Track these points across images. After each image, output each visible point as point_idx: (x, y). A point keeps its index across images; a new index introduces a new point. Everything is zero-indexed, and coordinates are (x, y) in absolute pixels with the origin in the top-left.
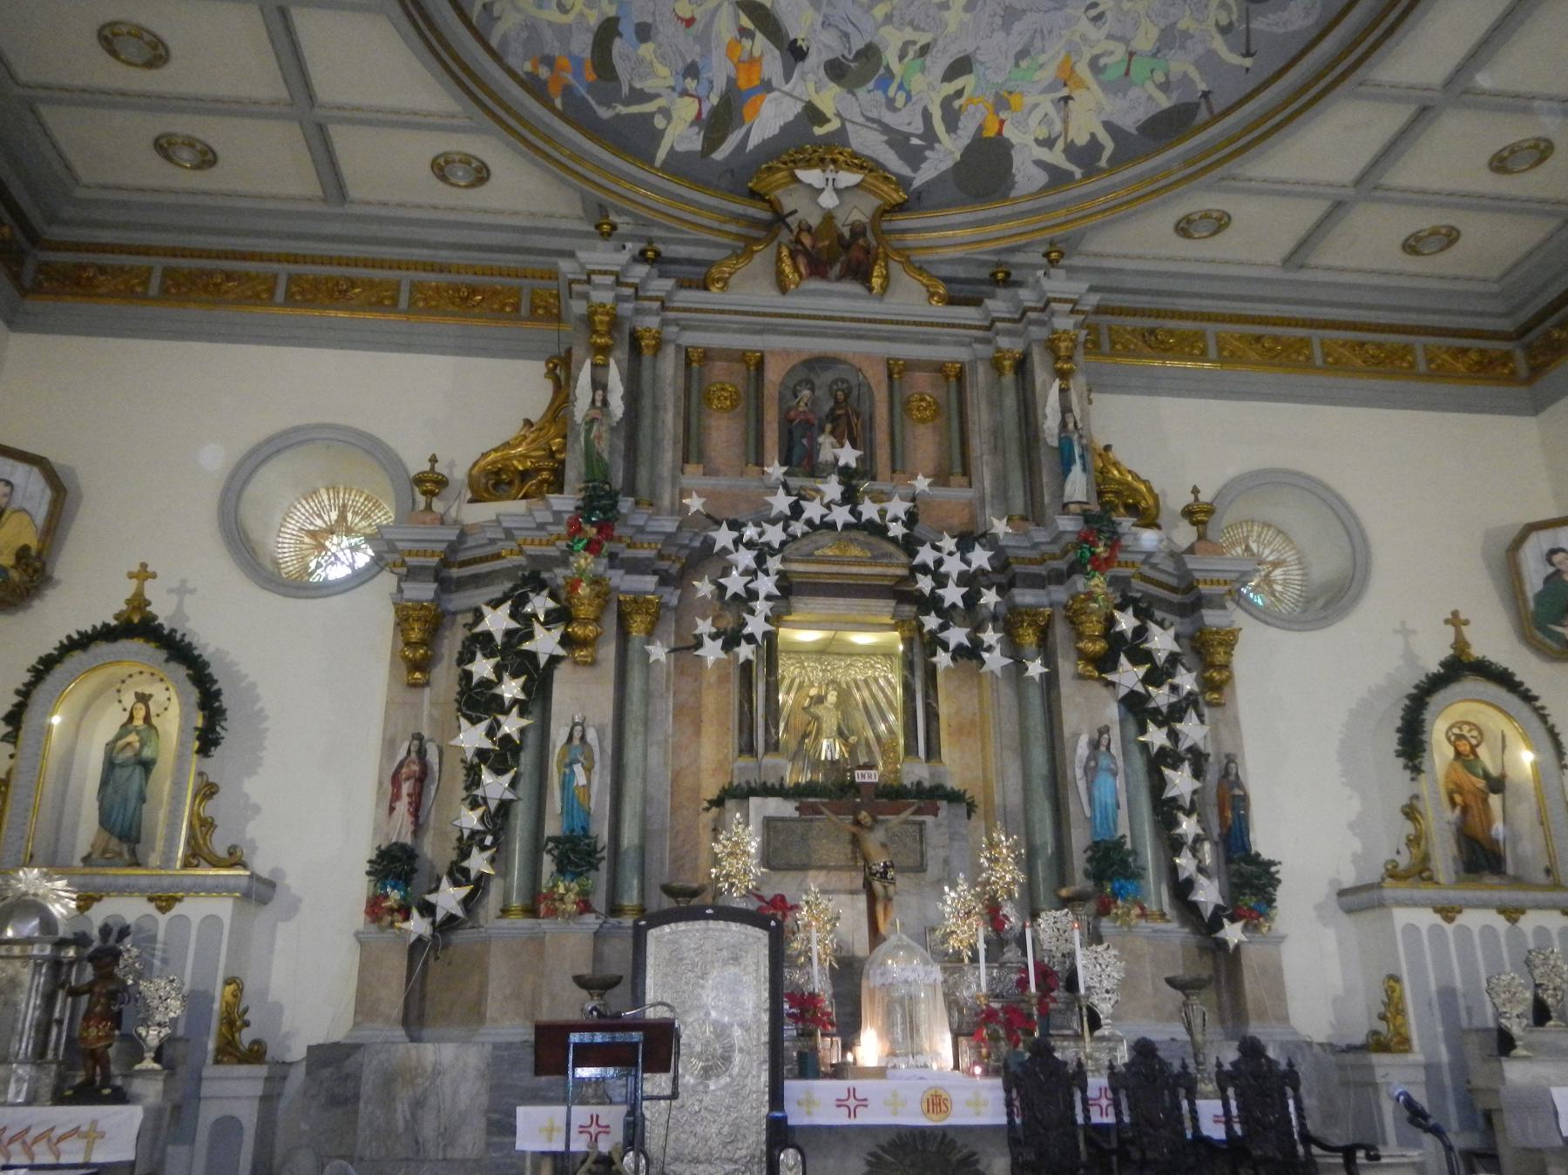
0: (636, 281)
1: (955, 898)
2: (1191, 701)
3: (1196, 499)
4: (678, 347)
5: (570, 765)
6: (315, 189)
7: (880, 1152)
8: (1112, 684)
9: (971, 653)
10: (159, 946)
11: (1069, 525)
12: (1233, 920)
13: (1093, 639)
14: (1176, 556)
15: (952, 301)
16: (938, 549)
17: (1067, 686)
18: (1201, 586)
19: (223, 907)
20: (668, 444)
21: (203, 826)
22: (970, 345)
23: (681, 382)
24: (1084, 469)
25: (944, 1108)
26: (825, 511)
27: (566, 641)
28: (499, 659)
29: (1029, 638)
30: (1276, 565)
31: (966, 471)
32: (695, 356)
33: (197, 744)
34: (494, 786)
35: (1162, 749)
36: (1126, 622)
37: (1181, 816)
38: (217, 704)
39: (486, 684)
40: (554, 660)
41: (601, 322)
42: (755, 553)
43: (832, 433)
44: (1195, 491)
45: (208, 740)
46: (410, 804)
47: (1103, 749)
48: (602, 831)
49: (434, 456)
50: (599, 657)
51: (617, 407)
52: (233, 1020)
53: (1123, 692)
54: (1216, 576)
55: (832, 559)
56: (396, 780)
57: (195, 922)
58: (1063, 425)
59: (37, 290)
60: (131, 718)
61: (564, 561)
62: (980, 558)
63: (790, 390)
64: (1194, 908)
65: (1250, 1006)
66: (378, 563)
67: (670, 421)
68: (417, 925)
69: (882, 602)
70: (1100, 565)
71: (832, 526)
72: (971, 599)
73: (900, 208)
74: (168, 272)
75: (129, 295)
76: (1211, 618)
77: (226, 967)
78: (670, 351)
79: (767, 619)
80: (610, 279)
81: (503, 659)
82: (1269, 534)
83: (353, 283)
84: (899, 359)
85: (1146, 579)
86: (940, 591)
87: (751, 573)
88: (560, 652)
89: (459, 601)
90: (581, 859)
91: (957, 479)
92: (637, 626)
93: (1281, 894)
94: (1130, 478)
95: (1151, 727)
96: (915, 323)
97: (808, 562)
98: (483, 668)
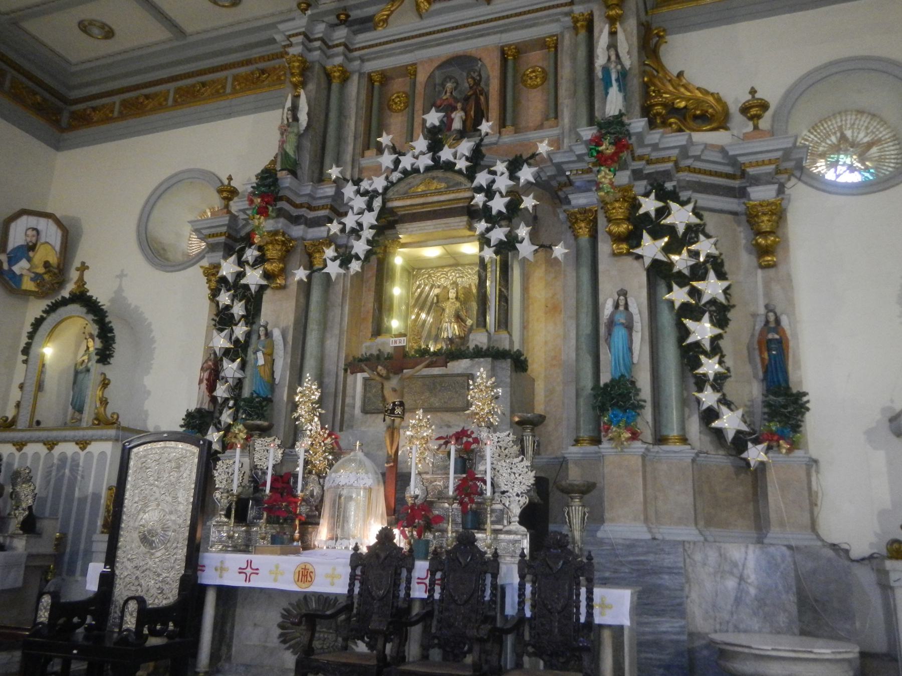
0: (320, 35)
3: (753, 97)
4: (361, 75)
5: (255, 353)
6: (169, 35)
7: (291, 609)
8: (639, 257)
10: (80, 468)
12: (756, 442)
13: (617, 222)
16: (494, 173)
18: (748, 170)
20: (351, 140)
21: (104, 402)
22: (558, 20)
23: (363, 96)
24: (623, 88)
25: (309, 579)
26: (414, 160)
27: (267, 275)
28: (232, 292)
30: (870, 145)
31: (556, 117)
32: (376, 77)
33: (98, 357)
35: (684, 305)
36: (649, 205)
37: (703, 358)
38: (109, 335)
39: (228, 307)
40: (262, 288)
41: (293, 67)
42: (367, 198)
43: (463, 109)
44: (753, 92)
45: (104, 356)
46: (207, 384)
47: (621, 308)
49: (230, 176)
50: (288, 283)
53: (647, 262)
54: (760, 157)
57: (96, 455)
58: (609, 59)
59: (70, 128)
60: (88, 348)
62: (526, 174)
64: (719, 433)
65: (773, 516)
67: (353, 124)
69: (458, 219)
71: (416, 170)
72: (513, 207)
74: (124, 104)
75: (108, 120)
76: (761, 194)
77: (108, 480)
78: (355, 78)
79: (369, 242)
80: (300, 39)
81: (235, 292)
82: (864, 120)
83: (204, 84)
84: (511, 45)
85: (690, 169)
86: (489, 203)
87: (361, 213)
88: (264, 282)
90: (252, 412)
91: (552, 122)
93: (812, 422)
94: (700, 95)
95: (675, 287)
96: (517, 15)
97: (403, 199)
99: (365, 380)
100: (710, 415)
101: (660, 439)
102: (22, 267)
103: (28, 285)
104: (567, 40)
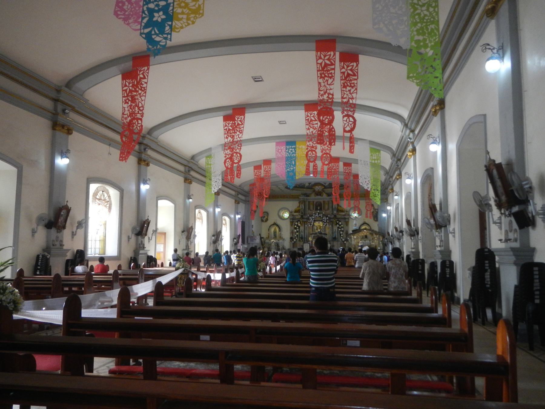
2: (343, 227)
9: (326, 225)
11: (333, 216)
14: (345, 215)
19: (282, 241)
21: (280, 236)
31: (329, 209)
36: (338, 222)
45: (280, 231)
51: (303, 208)
52: (283, 247)
62: (327, 218)
63: (316, 203)
67: (307, 207)
68: (293, 242)
70: (335, 219)
72: (326, 221)
73: (323, 189)
76: (347, 220)
89: (294, 220)
92: (305, 223)
99: (313, 236)
100: (342, 239)
101: (338, 241)
102: (264, 219)
103: (264, 221)
104: (330, 202)
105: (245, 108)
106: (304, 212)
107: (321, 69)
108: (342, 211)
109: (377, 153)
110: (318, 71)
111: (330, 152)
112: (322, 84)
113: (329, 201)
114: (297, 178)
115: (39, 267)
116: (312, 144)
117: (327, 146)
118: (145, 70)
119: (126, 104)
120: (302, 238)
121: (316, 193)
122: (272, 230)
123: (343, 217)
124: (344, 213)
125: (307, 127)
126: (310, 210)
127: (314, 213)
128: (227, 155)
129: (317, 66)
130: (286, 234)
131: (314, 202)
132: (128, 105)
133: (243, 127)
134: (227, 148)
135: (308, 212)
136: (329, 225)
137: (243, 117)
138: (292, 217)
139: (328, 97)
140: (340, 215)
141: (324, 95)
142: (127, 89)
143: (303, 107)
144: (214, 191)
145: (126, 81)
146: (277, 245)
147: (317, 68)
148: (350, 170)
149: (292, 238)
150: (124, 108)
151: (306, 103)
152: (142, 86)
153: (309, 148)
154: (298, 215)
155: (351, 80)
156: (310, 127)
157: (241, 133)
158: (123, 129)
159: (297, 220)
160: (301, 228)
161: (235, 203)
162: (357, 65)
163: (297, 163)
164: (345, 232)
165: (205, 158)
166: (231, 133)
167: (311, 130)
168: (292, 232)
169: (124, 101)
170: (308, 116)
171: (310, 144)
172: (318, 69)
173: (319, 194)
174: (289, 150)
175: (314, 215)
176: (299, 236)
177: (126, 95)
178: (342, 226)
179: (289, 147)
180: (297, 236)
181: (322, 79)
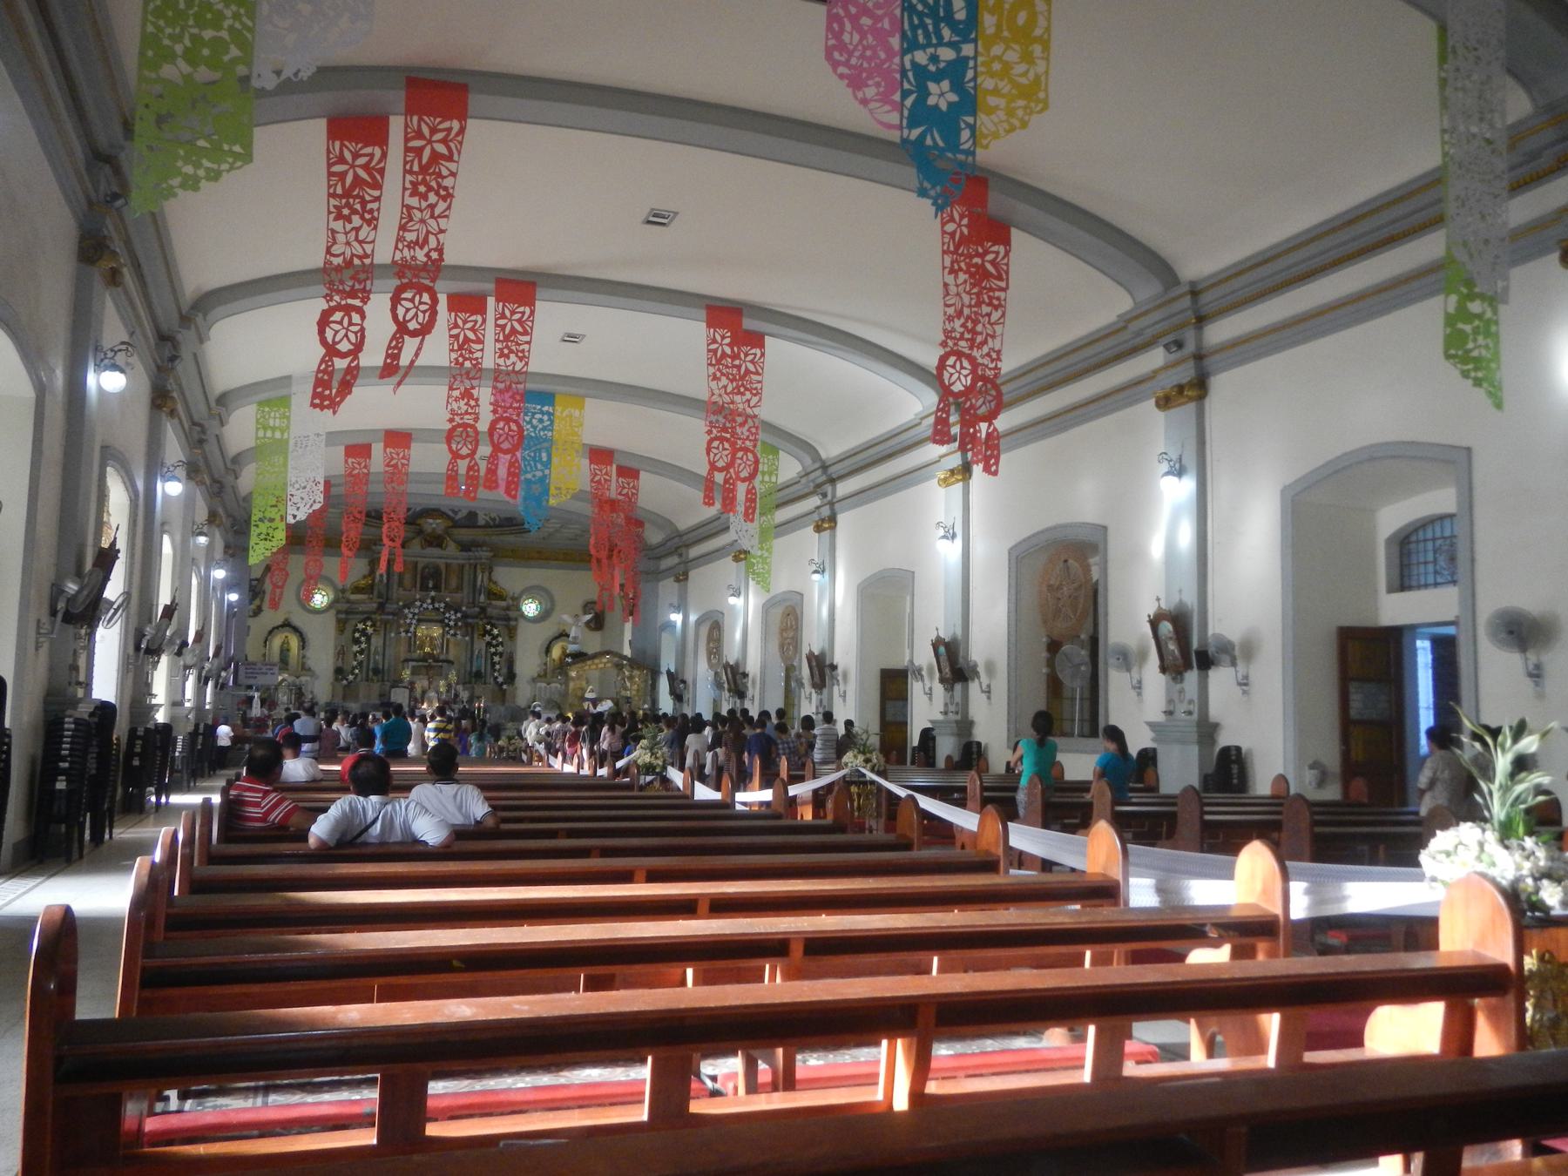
1: (442, 683)
2: (502, 643)
9: (455, 635)
11: (477, 609)
14: (508, 608)
15: (461, 551)
17: (476, 639)
19: (308, 678)
21: (303, 664)
29: (469, 629)
31: (462, 589)
34: (362, 657)
45: (303, 648)
48: (381, 667)
55: (429, 615)
56: (339, 654)
61: (375, 613)
62: (459, 615)
63: (424, 568)
66: (330, 606)
68: (345, 682)
70: (481, 619)
76: (512, 623)
89: (351, 617)
92: (388, 626)
98: (357, 635)
99: (413, 667)
100: (496, 678)
101: (485, 683)
104: (467, 568)
105: (533, 285)
106: (387, 591)
107: (952, 248)
108: (501, 597)
109: (771, 457)
110: (944, 252)
111: (755, 446)
112: (953, 289)
113: (462, 567)
114: (552, 502)
115: (65, 765)
116: (723, 421)
117: (748, 430)
118: (451, 137)
119: (341, 222)
120: (376, 671)
121: (425, 540)
122: (277, 642)
123: (503, 613)
124: (503, 604)
125: (712, 370)
126: (405, 590)
127: (418, 596)
128: (457, 414)
129: (943, 238)
130: (322, 657)
131: (417, 563)
132: (348, 227)
133: (529, 343)
134: (456, 393)
135: (397, 592)
136: (463, 636)
137: (528, 310)
138: (344, 606)
139: (963, 325)
140: (496, 607)
141: (956, 320)
142: (346, 173)
143: (703, 314)
144: (295, 517)
145: (342, 145)
146: (299, 693)
147: (943, 244)
148: (634, 487)
149: (339, 672)
150: (334, 232)
151: (708, 302)
152: (440, 180)
153: (714, 431)
154: (365, 602)
155: (991, 290)
156: (718, 374)
157: (521, 359)
158: (328, 301)
159: (362, 617)
160: (373, 640)
161: (225, 552)
162: (1007, 253)
163: (555, 459)
164: (504, 657)
165: (254, 407)
166: (471, 352)
167: (724, 381)
168: (341, 653)
169: (332, 209)
170: (714, 341)
171: (717, 421)
172: (945, 248)
173: (436, 541)
174: (533, 417)
175: (418, 603)
176: (365, 664)
177: (339, 191)
178: (500, 640)
179: (535, 408)
180: (360, 663)
181: (417, 198)
